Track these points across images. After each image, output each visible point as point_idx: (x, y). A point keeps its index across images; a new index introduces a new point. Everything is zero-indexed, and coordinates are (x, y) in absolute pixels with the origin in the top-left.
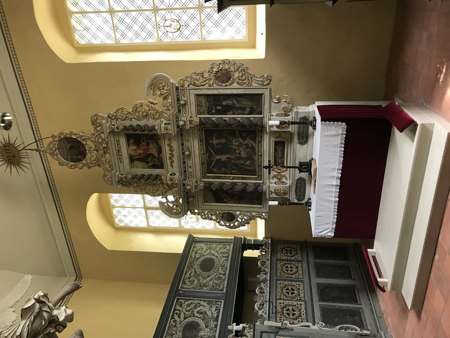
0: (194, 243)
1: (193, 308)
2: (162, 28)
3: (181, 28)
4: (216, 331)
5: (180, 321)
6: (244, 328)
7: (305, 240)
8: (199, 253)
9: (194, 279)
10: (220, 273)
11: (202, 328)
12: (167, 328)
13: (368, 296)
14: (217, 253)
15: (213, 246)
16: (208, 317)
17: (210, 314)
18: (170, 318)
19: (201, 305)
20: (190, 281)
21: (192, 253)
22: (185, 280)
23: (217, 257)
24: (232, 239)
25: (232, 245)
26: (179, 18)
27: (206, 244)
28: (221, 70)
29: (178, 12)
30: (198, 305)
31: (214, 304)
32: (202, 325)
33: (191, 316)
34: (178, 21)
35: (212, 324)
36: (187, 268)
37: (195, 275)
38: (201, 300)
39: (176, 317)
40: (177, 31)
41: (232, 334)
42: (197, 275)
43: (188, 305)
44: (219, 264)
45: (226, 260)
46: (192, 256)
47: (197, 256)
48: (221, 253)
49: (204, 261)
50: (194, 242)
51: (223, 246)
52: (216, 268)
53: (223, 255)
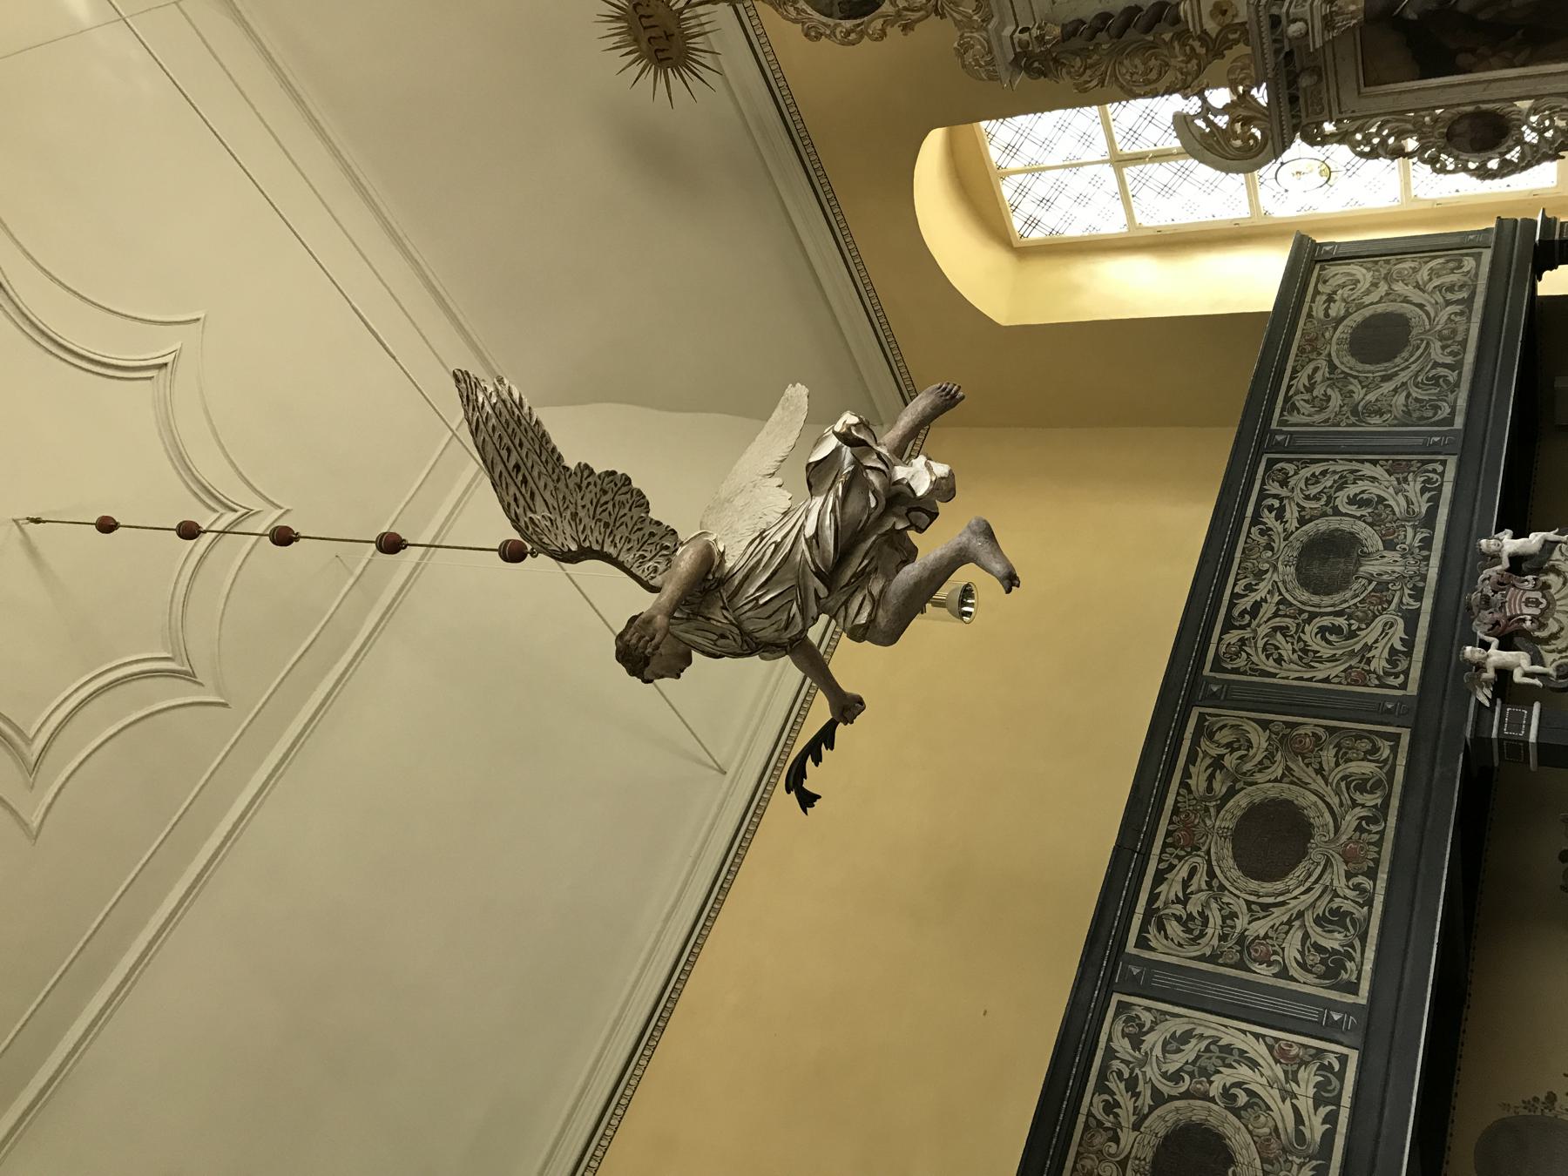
0: (1318, 267)
1: (1331, 487)
4: (1427, 558)
5: (1285, 530)
6: (1549, 547)
8: (1344, 300)
9: (1329, 389)
10: (1435, 362)
11: (1371, 550)
12: (1238, 554)
14: (1421, 293)
15: (1397, 266)
16: (1394, 514)
17: (1398, 505)
18: (1247, 522)
19: (1362, 478)
20: (1314, 398)
21: (1313, 301)
22: (1292, 396)
23: (1421, 306)
24: (1487, 230)
25: (1487, 255)
27: (1369, 265)
30: (1352, 477)
31: (1414, 472)
32: (1369, 543)
33: (1324, 514)
35: (1412, 537)
36: (1297, 355)
37: (1332, 376)
38: (1362, 462)
39: (1269, 519)
41: (1499, 568)
42: (1338, 378)
43: (1314, 479)
44: (1429, 330)
45: (1462, 313)
46: (1314, 313)
47: (1336, 309)
49: (1367, 323)
50: (1317, 262)
51: (1448, 262)
52: (1418, 348)
53: (1449, 296)
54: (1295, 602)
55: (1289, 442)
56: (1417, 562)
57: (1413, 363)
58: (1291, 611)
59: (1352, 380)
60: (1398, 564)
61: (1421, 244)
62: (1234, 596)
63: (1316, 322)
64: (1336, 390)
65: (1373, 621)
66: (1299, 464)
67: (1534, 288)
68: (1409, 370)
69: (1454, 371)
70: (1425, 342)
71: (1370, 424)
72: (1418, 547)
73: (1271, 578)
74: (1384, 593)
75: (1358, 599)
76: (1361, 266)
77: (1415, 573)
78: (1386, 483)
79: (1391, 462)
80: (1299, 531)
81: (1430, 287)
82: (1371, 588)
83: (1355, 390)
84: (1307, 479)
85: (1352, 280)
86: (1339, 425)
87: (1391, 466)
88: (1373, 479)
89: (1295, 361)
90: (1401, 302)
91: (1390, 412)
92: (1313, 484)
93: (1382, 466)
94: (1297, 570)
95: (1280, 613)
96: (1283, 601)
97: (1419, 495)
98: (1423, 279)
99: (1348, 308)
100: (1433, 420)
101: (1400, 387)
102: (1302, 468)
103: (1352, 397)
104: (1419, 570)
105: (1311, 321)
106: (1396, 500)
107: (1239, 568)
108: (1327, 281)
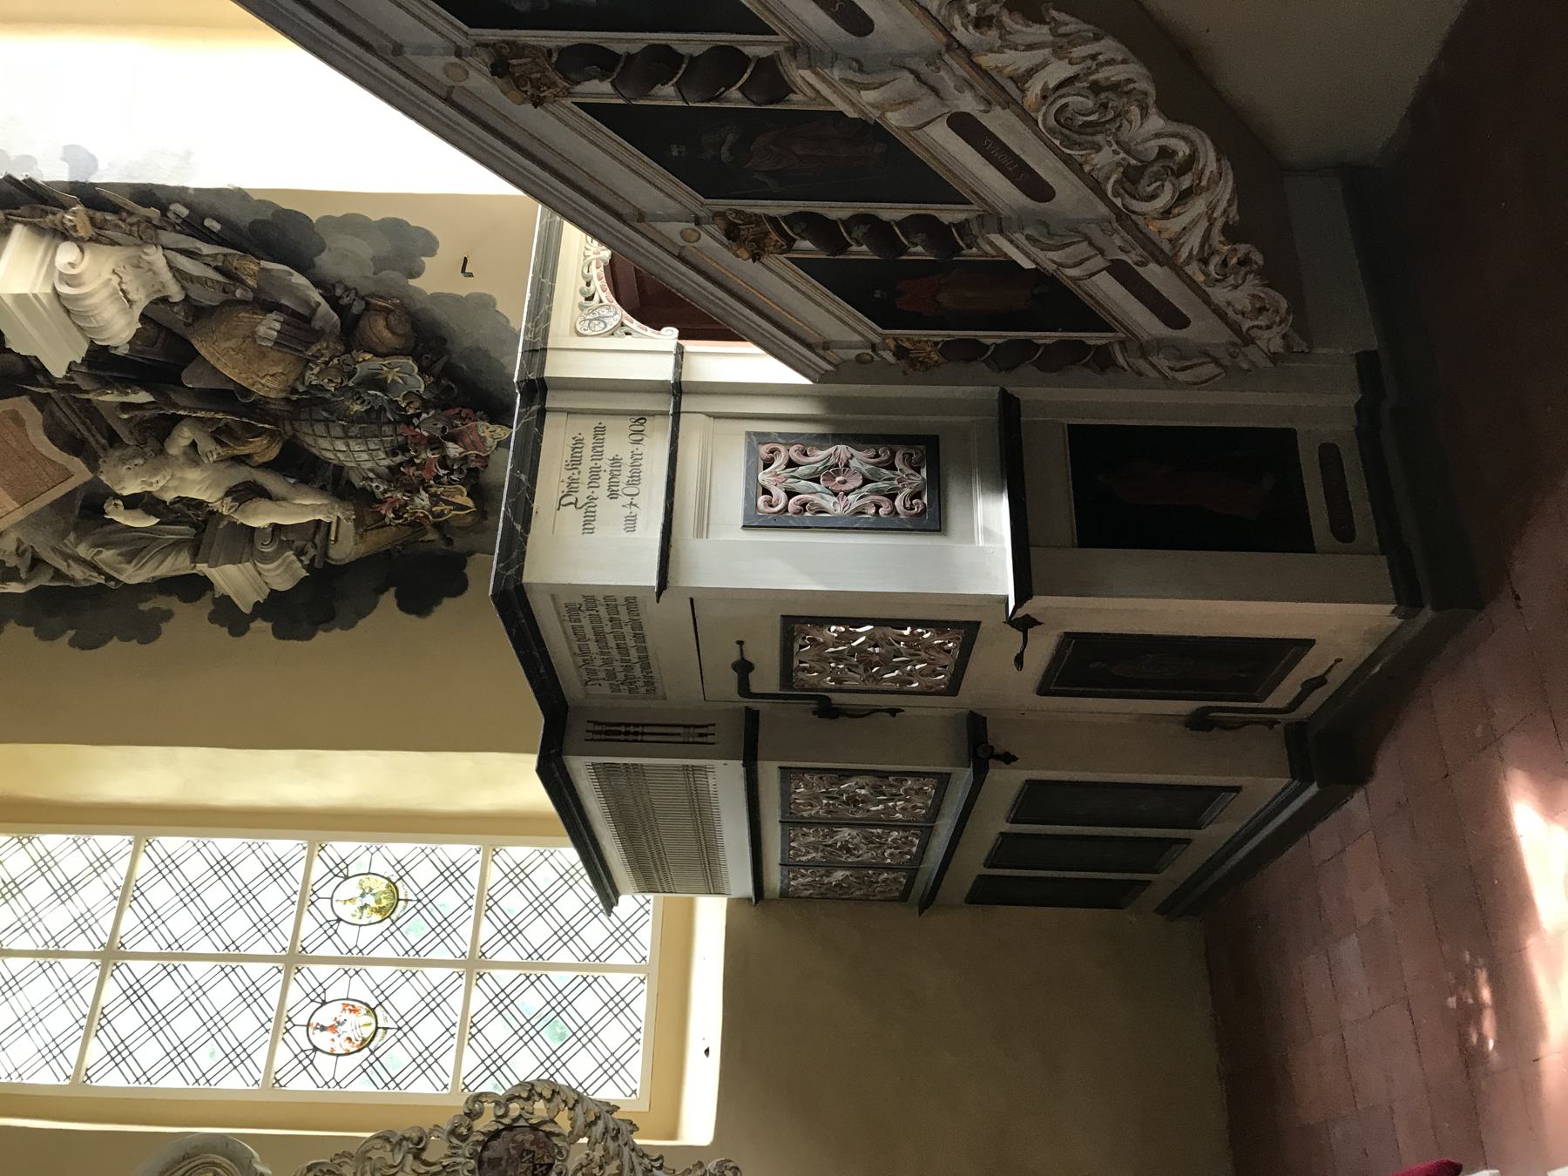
2: (299, 1033)
3: (377, 1039)
26: (381, 998)
28: (509, 1128)
29: (379, 973)
34: (373, 1010)
40: (359, 1051)
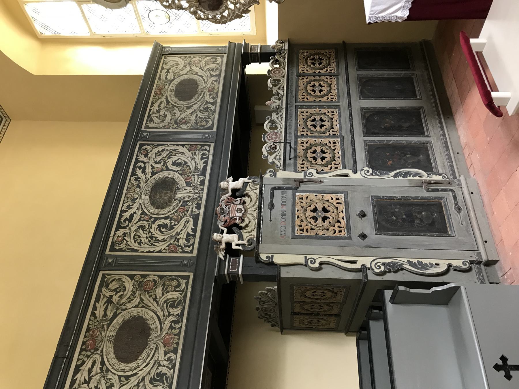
0: (163, 57)
1: (166, 157)
4: (202, 190)
5: (146, 178)
6: (245, 184)
7: (344, 42)
8: (173, 72)
9: (166, 112)
10: (207, 101)
11: (181, 186)
13: (441, 123)
14: (202, 71)
15: (194, 59)
16: (190, 170)
17: (192, 165)
18: (130, 174)
19: (178, 153)
20: (160, 116)
21: (161, 72)
22: (151, 115)
23: (202, 77)
24: (225, 47)
25: (225, 56)
27: (183, 58)
30: (174, 152)
31: (198, 150)
32: (180, 183)
33: (162, 170)
35: (197, 180)
36: (154, 96)
37: (168, 106)
38: (178, 145)
39: (139, 172)
41: (227, 195)
42: (170, 107)
43: (158, 154)
44: (204, 88)
45: (216, 81)
46: (161, 77)
47: (170, 76)
48: (209, 71)
49: (181, 83)
50: (163, 55)
51: (212, 58)
52: (201, 95)
53: (212, 73)
54: (148, 213)
55: (149, 136)
56: (198, 192)
57: (199, 101)
58: (146, 218)
59: (175, 108)
60: (191, 193)
61: (202, 50)
62: (123, 211)
63: (162, 82)
64: (169, 112)
65: (180, 220)
66: (153, 146)
67: (243, 72)
68: (197, 104)
69: (213, 106)
70: (203, 92)
71: (182, 128)
72: (199, 184)
73: (139, 202)
74: (186, 207)
75: (175, 210)
76: (180, 58)
77: (198, 196)
78: (187, 155)
79: (189, 145)
80: (151, 178)
81: (205, 69)
82: (180, 205)
83: (176, 112)
84: (156, 154)
85: (176, 64)
86: (169, 128)
87: (190, 148)
88: (183, 153)
89: (153, 98)
90: (195, 74)
91: (190, 123)
92: (158, 156)
93: (186, 147)
94: (150, 197)
95: (142, 219)
96: (143, 213)
97: (200, 161)
98: (202, 65)
99: (175, 76)
100: (206, 127)
101: (194, 112)
102: (154, 148)
103: (175, 115)
104: (199, 195)
105: (160, 81)
106: (191, 163)
107: (125, 198)
108: (167, 63)
